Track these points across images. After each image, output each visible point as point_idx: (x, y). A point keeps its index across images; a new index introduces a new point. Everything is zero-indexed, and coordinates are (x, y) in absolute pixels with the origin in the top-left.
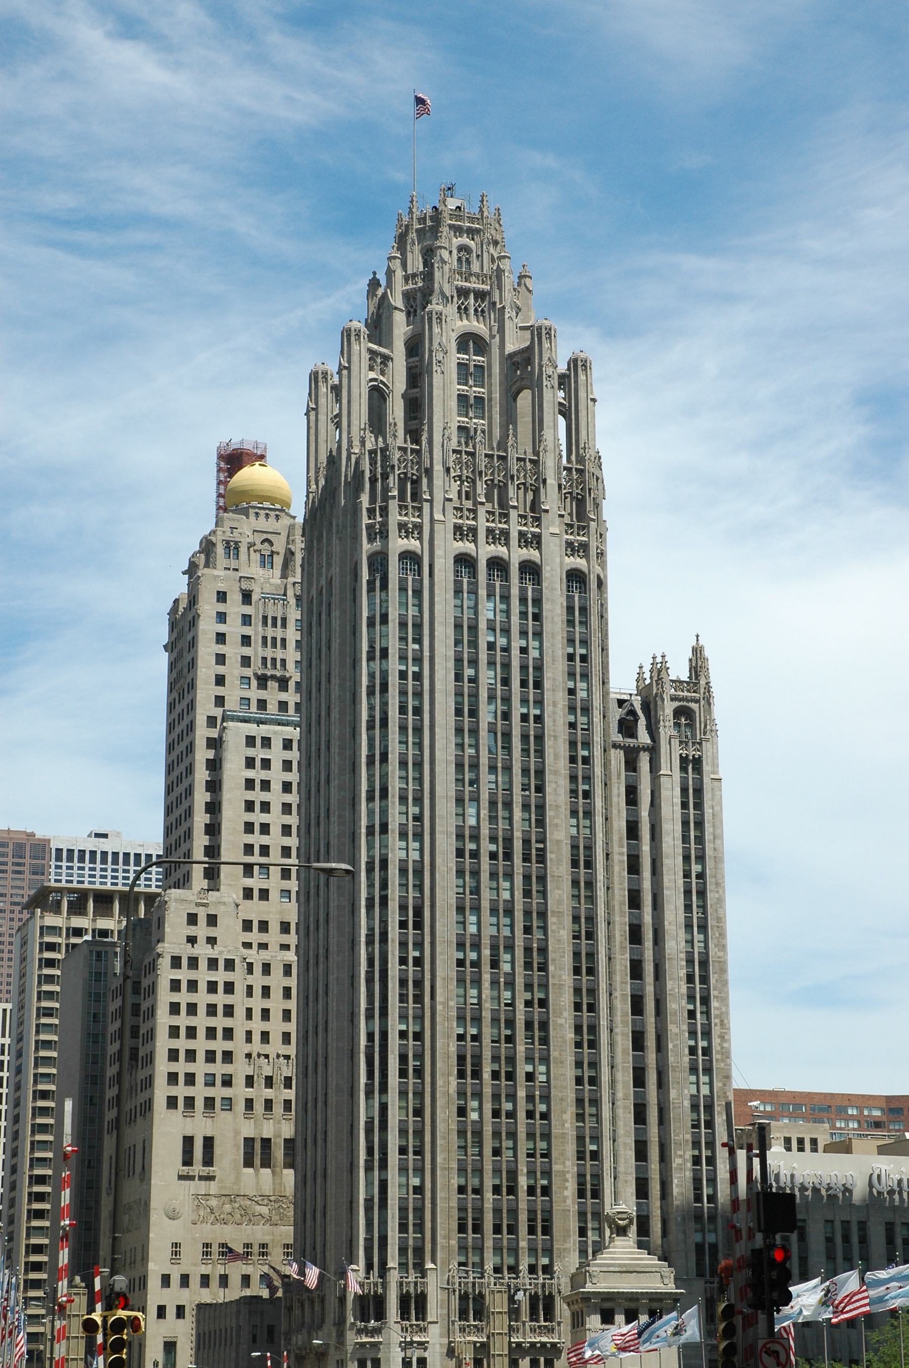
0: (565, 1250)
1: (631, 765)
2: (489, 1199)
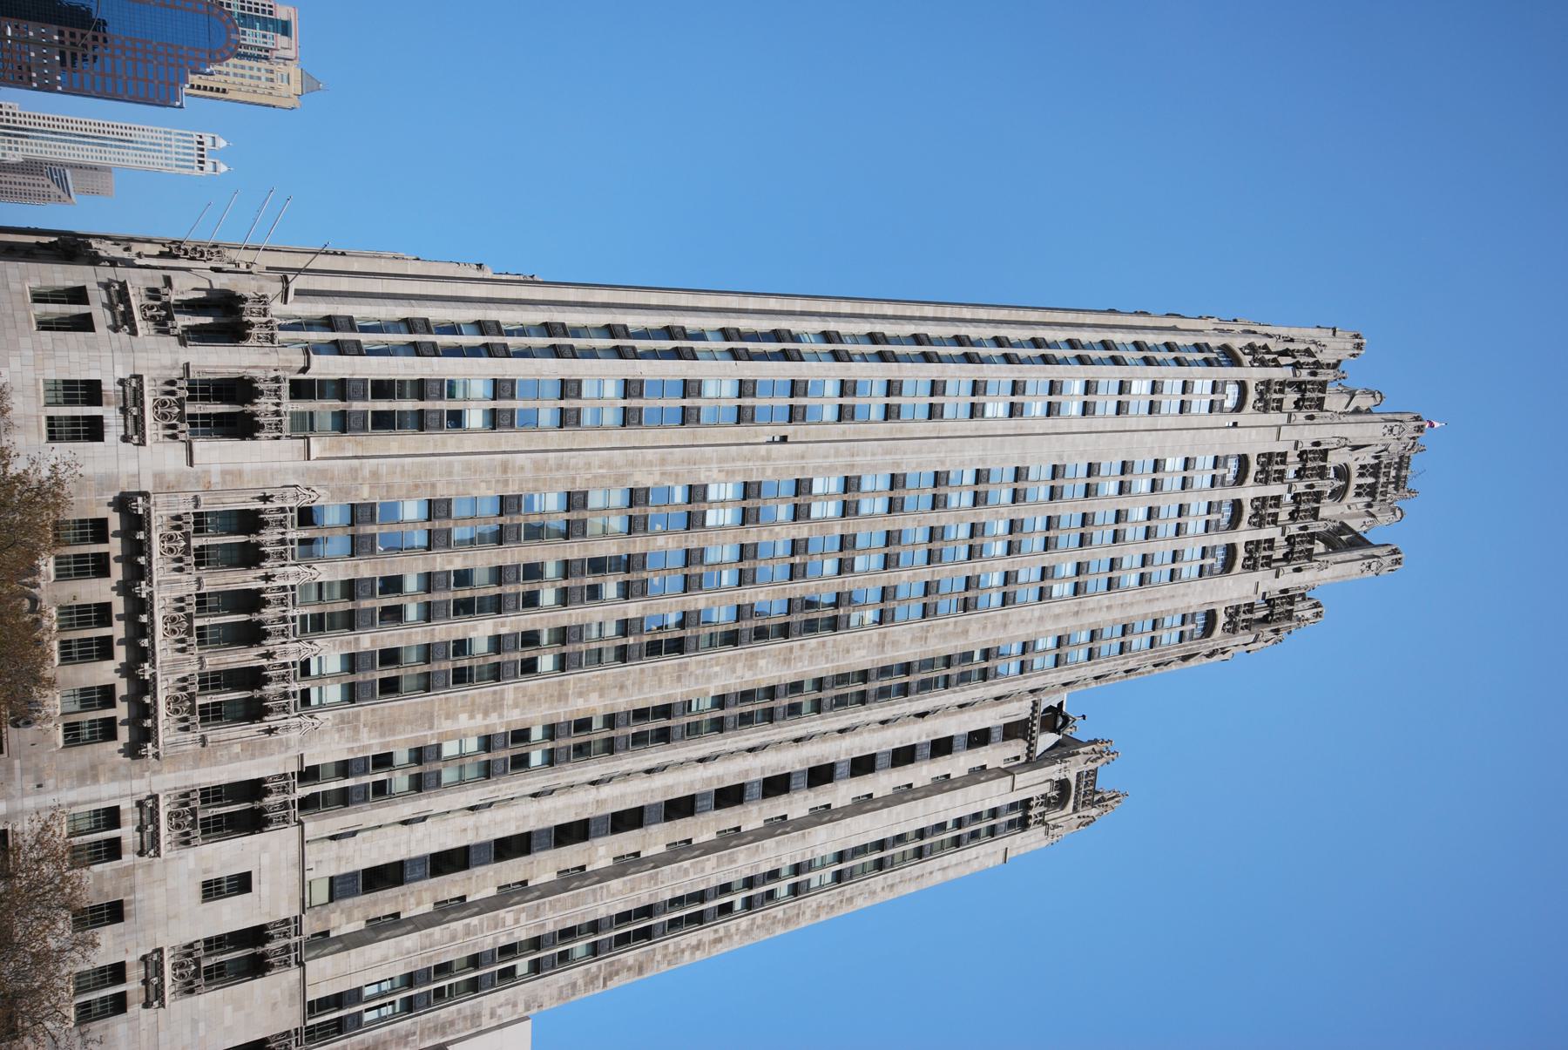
0: (356, 730)
1: (1012, 731)
2: (450, 562)
